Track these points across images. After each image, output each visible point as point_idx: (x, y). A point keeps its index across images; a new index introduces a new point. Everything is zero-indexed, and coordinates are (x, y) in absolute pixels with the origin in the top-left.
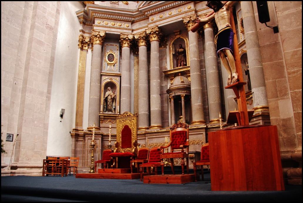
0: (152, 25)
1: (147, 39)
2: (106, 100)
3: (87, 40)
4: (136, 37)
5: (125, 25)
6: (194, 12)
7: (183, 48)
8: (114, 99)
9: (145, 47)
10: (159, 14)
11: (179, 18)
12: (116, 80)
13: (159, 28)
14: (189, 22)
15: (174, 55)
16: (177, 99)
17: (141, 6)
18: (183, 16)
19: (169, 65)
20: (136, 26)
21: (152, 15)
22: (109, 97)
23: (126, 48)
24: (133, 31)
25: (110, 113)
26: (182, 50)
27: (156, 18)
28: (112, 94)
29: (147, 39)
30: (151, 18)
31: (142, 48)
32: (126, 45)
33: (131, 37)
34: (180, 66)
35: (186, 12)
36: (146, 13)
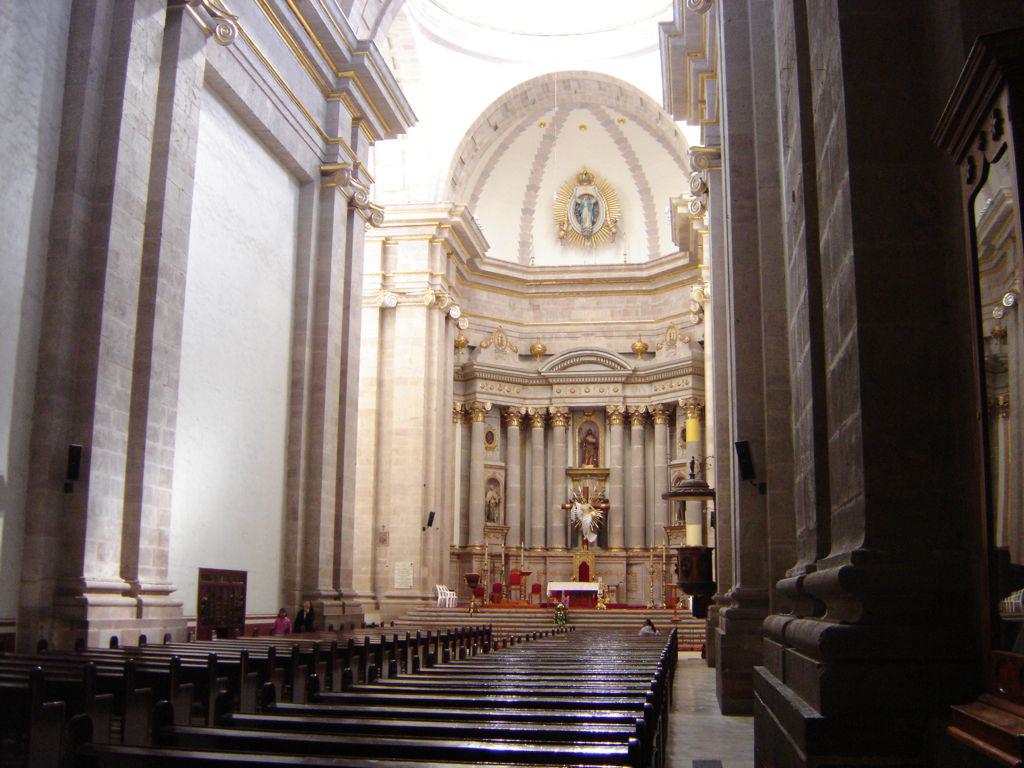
0: (559, 400)
1: (548, 420)
2: (488, 505)
3: (459, 409)
4: (531, 412)
5: (515, 389)
6: (621, 399)
7: (594, 437)
8: (497, 504)
9: (542, 429)
11: (600, 403)
12: (501, 479)
13: (570, 408)
15: (581, 445)
19: (573, 460)
22: (493, 501)
23: (514, 427)
24: (525, 399)
25: (493, 524)
26: (594, 440)
27: (565, 390)
28: (496, 496)
29: (548, 420)
31: (538, 427)
32: (516, 423)
33: (523, 412)
34: (588, 464)
36: (551, 381)
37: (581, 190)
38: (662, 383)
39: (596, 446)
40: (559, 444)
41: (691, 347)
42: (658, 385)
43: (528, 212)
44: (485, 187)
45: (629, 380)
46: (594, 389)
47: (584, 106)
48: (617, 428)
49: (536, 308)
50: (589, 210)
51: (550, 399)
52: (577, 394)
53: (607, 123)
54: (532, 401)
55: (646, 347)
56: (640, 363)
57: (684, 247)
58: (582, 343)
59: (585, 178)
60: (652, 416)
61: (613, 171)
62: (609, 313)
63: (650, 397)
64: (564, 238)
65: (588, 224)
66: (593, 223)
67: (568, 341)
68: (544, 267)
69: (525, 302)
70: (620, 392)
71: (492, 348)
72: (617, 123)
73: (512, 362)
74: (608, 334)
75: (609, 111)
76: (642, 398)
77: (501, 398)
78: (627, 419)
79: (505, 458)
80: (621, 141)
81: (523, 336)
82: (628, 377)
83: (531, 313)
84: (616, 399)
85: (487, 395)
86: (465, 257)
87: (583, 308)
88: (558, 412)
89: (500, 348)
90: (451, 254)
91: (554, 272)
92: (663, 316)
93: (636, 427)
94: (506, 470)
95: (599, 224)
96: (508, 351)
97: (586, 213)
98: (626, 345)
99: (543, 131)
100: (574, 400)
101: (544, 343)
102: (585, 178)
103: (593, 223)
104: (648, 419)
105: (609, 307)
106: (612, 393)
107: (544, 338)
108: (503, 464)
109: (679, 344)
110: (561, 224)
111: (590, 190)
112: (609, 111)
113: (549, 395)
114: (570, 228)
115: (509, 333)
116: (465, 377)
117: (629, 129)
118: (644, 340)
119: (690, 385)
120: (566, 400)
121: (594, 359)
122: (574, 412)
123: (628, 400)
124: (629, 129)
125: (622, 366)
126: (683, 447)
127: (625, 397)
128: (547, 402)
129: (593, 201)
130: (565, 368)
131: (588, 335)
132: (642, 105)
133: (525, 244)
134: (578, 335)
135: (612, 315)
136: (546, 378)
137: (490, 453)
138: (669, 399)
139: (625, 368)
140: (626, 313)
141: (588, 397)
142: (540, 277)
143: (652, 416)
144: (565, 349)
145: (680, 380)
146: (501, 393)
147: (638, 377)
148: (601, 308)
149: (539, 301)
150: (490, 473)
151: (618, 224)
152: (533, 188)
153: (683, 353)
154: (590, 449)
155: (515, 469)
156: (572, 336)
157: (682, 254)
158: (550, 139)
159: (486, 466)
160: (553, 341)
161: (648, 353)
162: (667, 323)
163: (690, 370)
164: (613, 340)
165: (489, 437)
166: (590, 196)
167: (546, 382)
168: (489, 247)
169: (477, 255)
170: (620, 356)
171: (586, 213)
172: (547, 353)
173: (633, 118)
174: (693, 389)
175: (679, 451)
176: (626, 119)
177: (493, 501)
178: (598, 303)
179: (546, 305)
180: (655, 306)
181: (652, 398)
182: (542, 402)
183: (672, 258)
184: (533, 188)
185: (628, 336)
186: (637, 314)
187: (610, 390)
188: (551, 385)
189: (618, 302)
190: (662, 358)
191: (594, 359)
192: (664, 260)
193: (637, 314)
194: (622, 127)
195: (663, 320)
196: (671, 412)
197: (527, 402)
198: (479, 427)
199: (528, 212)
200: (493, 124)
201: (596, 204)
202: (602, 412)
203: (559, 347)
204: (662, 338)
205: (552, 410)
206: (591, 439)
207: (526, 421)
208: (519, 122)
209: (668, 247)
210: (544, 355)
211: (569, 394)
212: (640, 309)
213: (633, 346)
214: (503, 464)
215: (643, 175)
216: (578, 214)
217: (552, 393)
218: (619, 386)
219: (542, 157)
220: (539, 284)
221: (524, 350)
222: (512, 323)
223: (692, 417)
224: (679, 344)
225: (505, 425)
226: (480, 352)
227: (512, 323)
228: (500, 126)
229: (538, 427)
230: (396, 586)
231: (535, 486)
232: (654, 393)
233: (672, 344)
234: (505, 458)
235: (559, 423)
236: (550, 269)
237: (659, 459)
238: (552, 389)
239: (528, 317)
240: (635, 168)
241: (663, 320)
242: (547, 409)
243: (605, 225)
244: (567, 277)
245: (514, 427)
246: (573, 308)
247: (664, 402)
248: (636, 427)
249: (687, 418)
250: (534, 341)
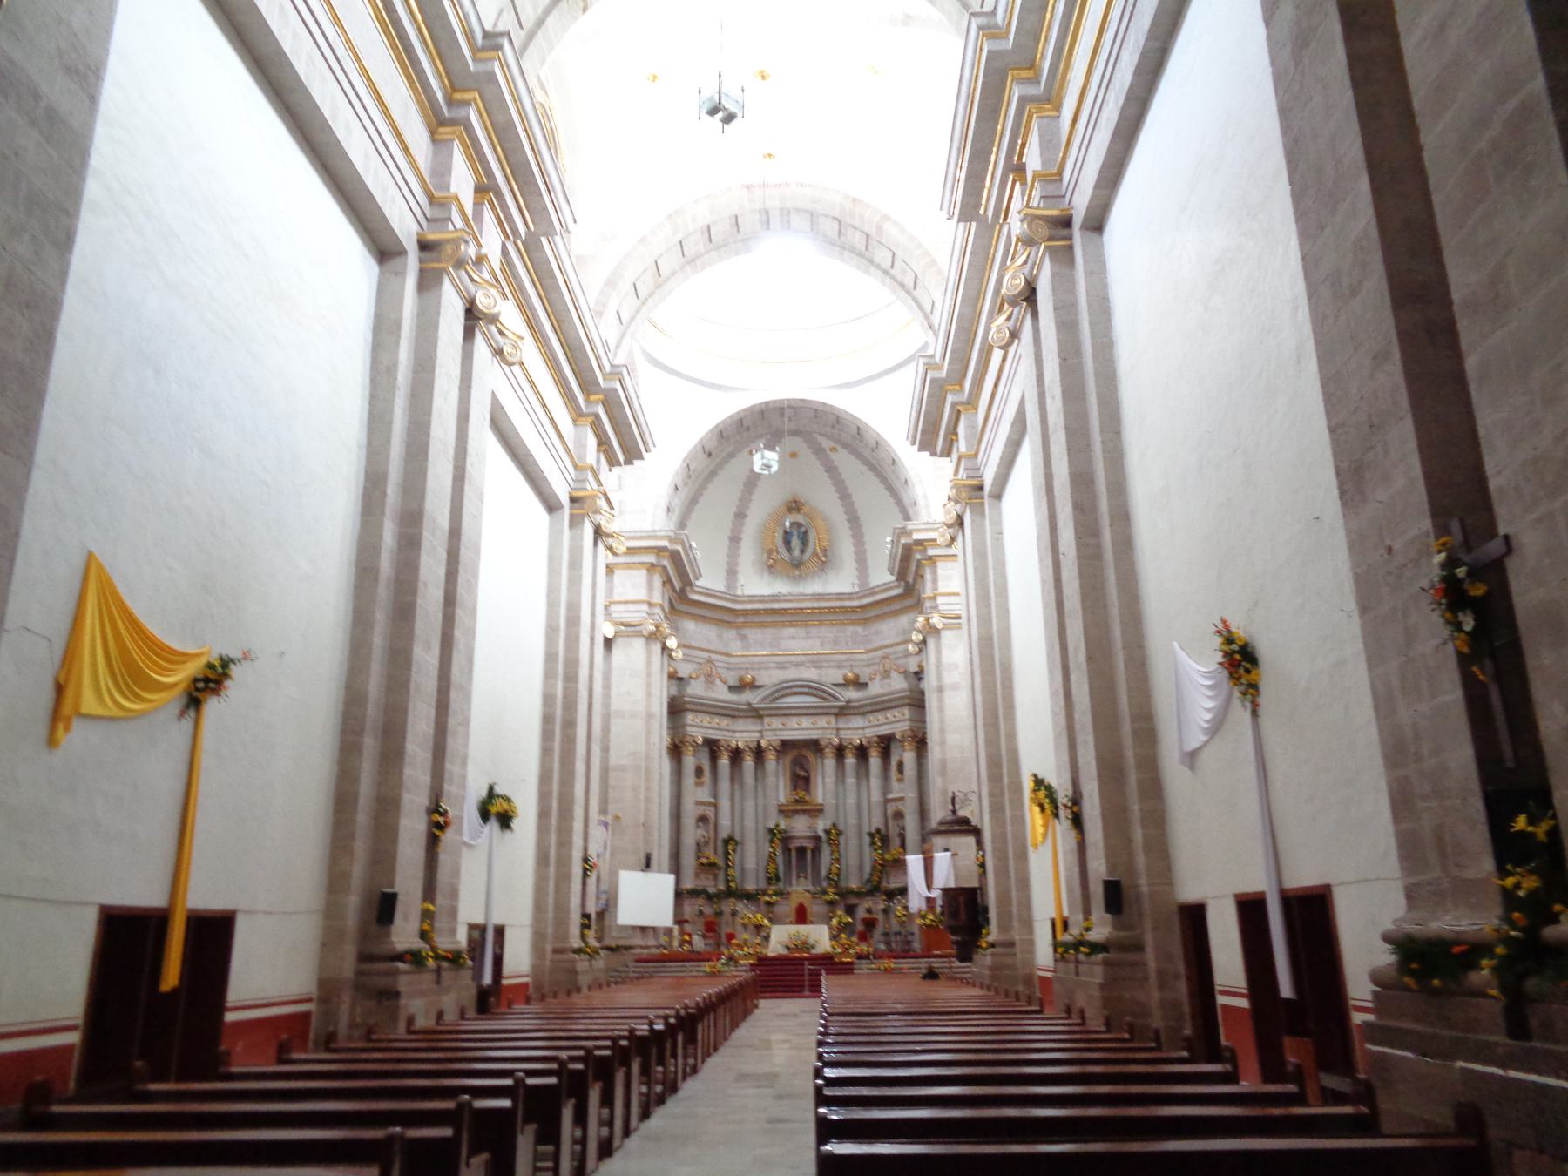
0: (770, 733)
1: (759, 752)
5: (725, 722)
6: (835, 732)
7: (806, 771)
8: (706, 843)
11: (813, 735)
12: (710, 812)
13: (781, 741)
14: (827, 746)
16: (801, 851)
18: (820, 732)
20: (741, 725)
21: (770, 715)
23: (724, 762)
24: (734, 731)
26: (805, 774)
27: (776, 723)
29: (759, 752)
30: (766, 720)
31: (749, 762)
33: (733, 744)
36: (762, 712)
38: (876, 714)
39: (807, 780)
40: (771, 779)
41: (906, 678)
42: (871, 717)
43: (735, 540)
44: (694, 516)
45: (843, 711)
46: (806, 722)
47: (795, 433)
48: (830, 763)
49: (743, 638)
51: (761, 732)
52: (788, 726)
53: (818, 451)
54: (742, 734)
55: (857, 677)
56: (852, 694)
57: (902, 576)
58: (792, 674)
59: (794, 506)
60: (867, 748)
61: (824, 500)
62: (818, 642)
63: (863, 728)
64: (772, 567)
65: (797, 553)
66: (803, 551)
67: (778, 672)
68: (753, 596)
69: (732, 633)
70: (833, 724)
71: (702, 679)
72: (828, 451)
73: (721, 693)
74: (817, 665)
75: (822, 440)
76: (858, 730)
77: (710, 731)
78: (840, 751)
79: (715, 796)
80: (831, 470)
81: (732, 666)
82: (841, 708)
83: (739, 643)
84: (829, 732)
85: (698, 727)
86: (677, 585)
88: (748, 746)
89: (709, 679)
90: (667, 582)
91: (762, 602)
92: (875, 645)
93: (850, 760)
94: (715, 805)
95: (809, 551)
96: (718, 682)
97: (795, 542)
98: (837, 675)
100: (785, 733)
101: (753, 673)
102: (794, 506)
103: (803, 551)
104: (862, 752)
105: (819, 637)
106: (826, 725)
107: (753, 669)
108: (713, 800)
109: (894, 675)
110: (770, 552)
111: (800, 518)
112: (822, 440)
113: (759, 728)
115: (718, 664)
116: (676, 709)
117: (842, 459)
118: (857, 671)
119: (907, 716)
120: (778, 733)
121: (806, 690)
122: (786, 746)
123: (842, 732)
124: (842, 459)
125: (834, 697)
126: (900, 780)
127: (838, 729)
128: (757, 735)
129: (803, 529)
130: (777, 699)
131: (798, 665)
132: (858, 434)
133: (732, 573)
134: (788, 665)
135: (822, 645)
136: (756, 710)
137: (700, 789)
138: (884, 730)
140: (836, 643)
141: (800, 729)
142: (749, 606)
143: (867, 748)
144: (776, 681)
145: (896, 712)
146: (712, 726)
147: (854, 708)
148: (811, 638)
149: (746, 631)
150: (701, 810)
151: (828, 552)
152: (740, 516)
153: (898, 684)
154: (801, 781)
155: (725, 804)
156: (781, 666)
157: (896, 583)
159: (699, 803)
160: (763, 672)
161: (858, 684)
162: (880, 653)
163: (907, 701)
164: (823, 671)
165: (699, 771)
166: (799, 525)
167: (756, 714)
168: (701, 575)
169: (690, 584)
170: (835, 688)
171: (795, 542)
172: (757, 683)
173: (845, 446)
174: (911, 720)
175: (895, 785)
176: (838, 447)
177: (702, 840)
178: (807, 633)
179: (753, 634)
180: (866, 636)
181: (867, 731)
182: (752, 734)
183: (886, 587)
184: (740, 516)
185: (839, 667)
186: (847, 643)
187: (822, 722)
188: (761, 717)
189: (827, 632)
190: (876, 688)
191: (806, 690)
192: (876, 589)
193: (847, 643)
194: (833, 456)
195: (875, 650)
196: (886, 744)
197: (737, 735)
198: (689, 761)
199: (735, 540)
200: (707, 450)
201: (806, 533)
202: (815, 746)
203: (770, 677)
204: (876, 667)
205: (763, 743)
206: (803, 773)
207: (736, 755)
208: (730, 449)
209: (882, 576)
210: (753, 686)
211: (781, 726)
212: (849, 639)
213: (845, 678)
214: (713, 800)
215: (852, 504)
216: (787, 543)
217: (762, 724)
218: (832, 719)
220: (745, 613)
221: (733, 682)
222: (720, 653)
223: (911, 750)
224: (894, 675)
225: (714, 758)
226: (689, 683)
227: (720, 653)
228: (714, 454)
229: (749, 762)
230: (614, 934)
231: (746, 823)
232: (867, 724)
233: (886, 675)
234: (715, 796)
235: (771, 757)
236: (760, 598)
237: (876, 796)
238: (762, 720)
239: (736, 647)
240: (845, 496)
241: (875, 650)
242: (759, 743)
243: (815, 554)
244: (776, 606)
245: (724, 762)
246: (781, 638)
247: (878, 734)
248: (850, 760)
249: (904, 750)
250: (743, 673)
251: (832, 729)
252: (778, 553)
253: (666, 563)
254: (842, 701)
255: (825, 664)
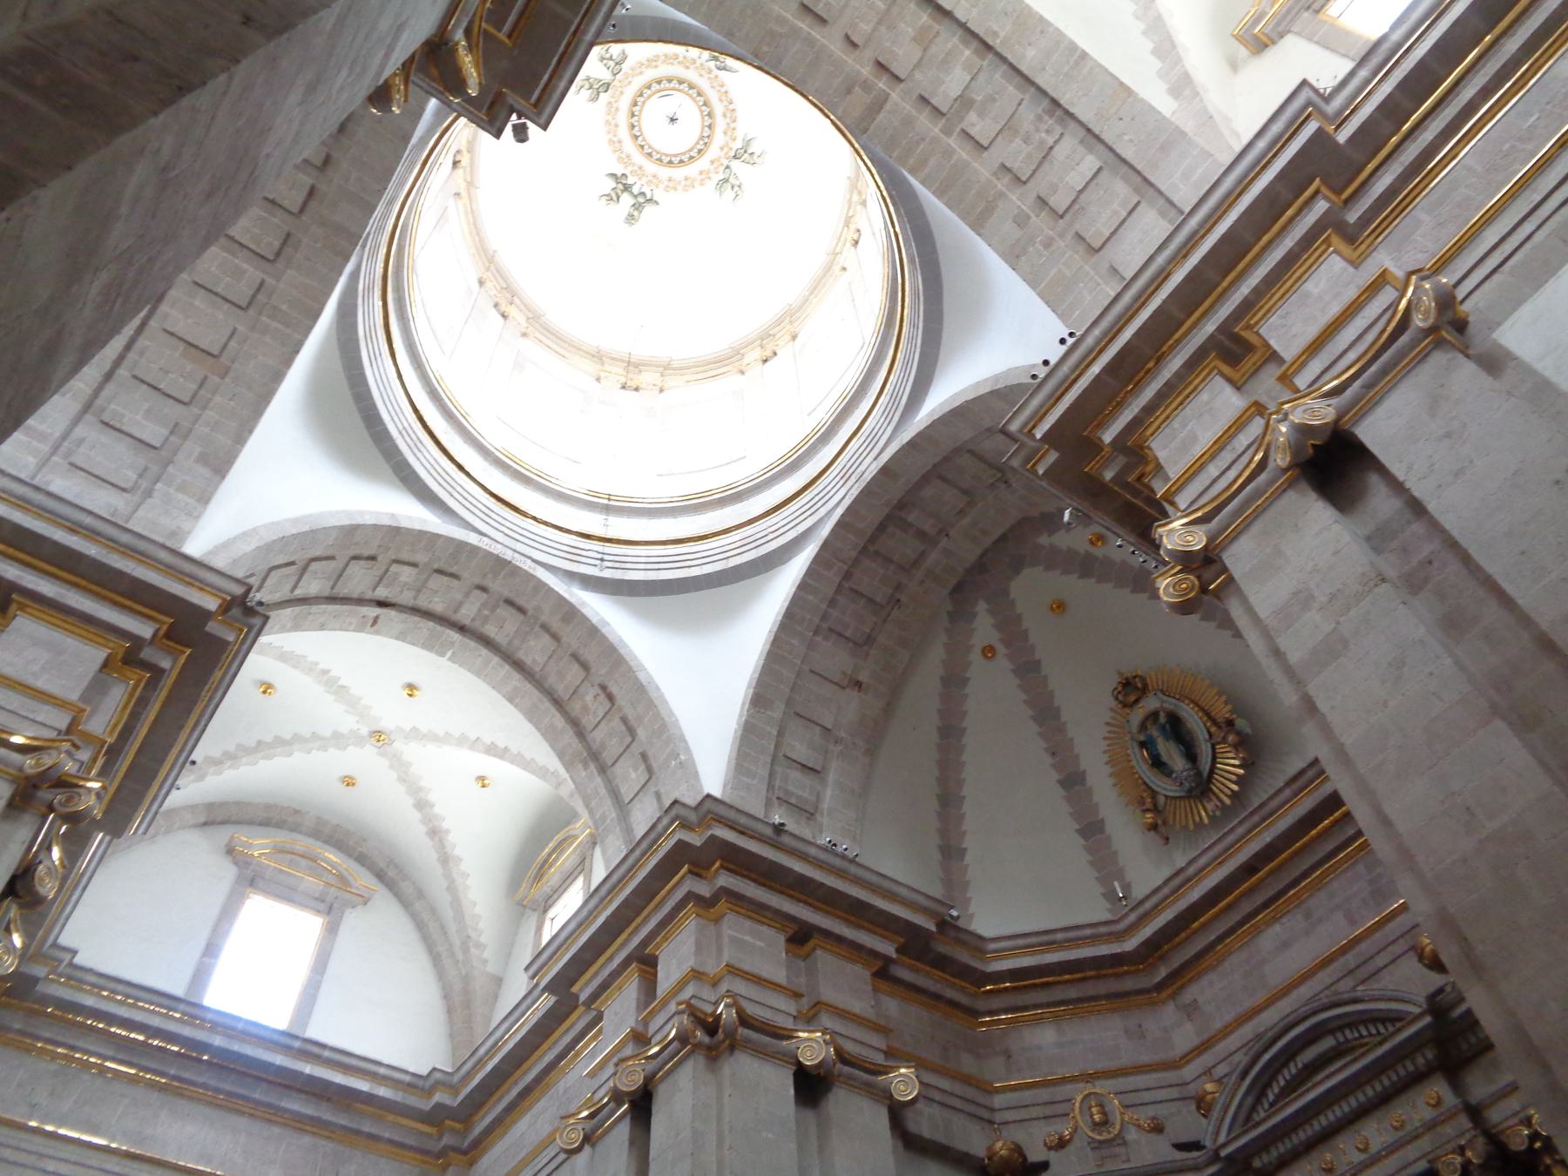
6: (1464, 1122)
10: (1315, 1154)
17: (1222, 1139)
18: (1424, 1144)
35: (1430, 1126)
36: (1257, 1163)
37: (1138, 715)
43: (1092, 829)
49: (1191, 1010)
50: (1167, 739)
59: (1131, 689)
65: (1178, 763)
66: (1191, 756)
70: (1450, 1099)
83: (1189, 1026)
87: (1285, 945)
99: (1002, 663)
102: (1131, 689)
103: (1191, 756)
106: (1428, 1114)
111: (1151, 703)
114: (1161, 800)
121: (1327, 1043)
129: (1162, 719)
139: (1395, 1019)
149: (1188, 996)
152: (1073, 781)
158: (1028, 670)
166: (1154, 715)
178: (1308, 915)
184: (1073, 781)
191: (1327, 1043)
199: (1092, 829)
216: (1158, 763)
219: (1046, 714)
251: (1450, 1116)
252: (1154, 794)
253: (725, 880)
254: (1420, 1016)
255: (1380, 960)
